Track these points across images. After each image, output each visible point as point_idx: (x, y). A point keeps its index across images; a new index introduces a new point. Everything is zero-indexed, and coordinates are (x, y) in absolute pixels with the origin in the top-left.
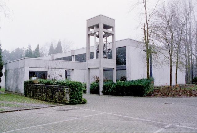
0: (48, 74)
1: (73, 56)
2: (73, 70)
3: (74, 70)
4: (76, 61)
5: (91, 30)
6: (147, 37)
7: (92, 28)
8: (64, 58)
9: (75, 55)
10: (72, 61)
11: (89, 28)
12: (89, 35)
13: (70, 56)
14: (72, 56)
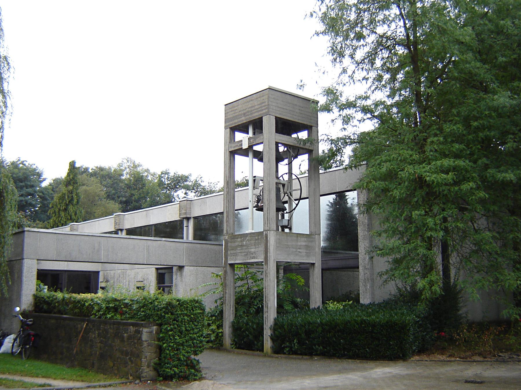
0: (101, 279)
1: (188, 219)
2: (181, 268)
3: (186, 268)
4: (195, 239)
5: (239, 136)
6: (263, 105)
7: (244, 129)
8: (155, 225)
9: (126, 229)
10: (183, 238)
11: (233, 130)
12: (233, 154)
13: (177, 218)
14: (181, 222)
